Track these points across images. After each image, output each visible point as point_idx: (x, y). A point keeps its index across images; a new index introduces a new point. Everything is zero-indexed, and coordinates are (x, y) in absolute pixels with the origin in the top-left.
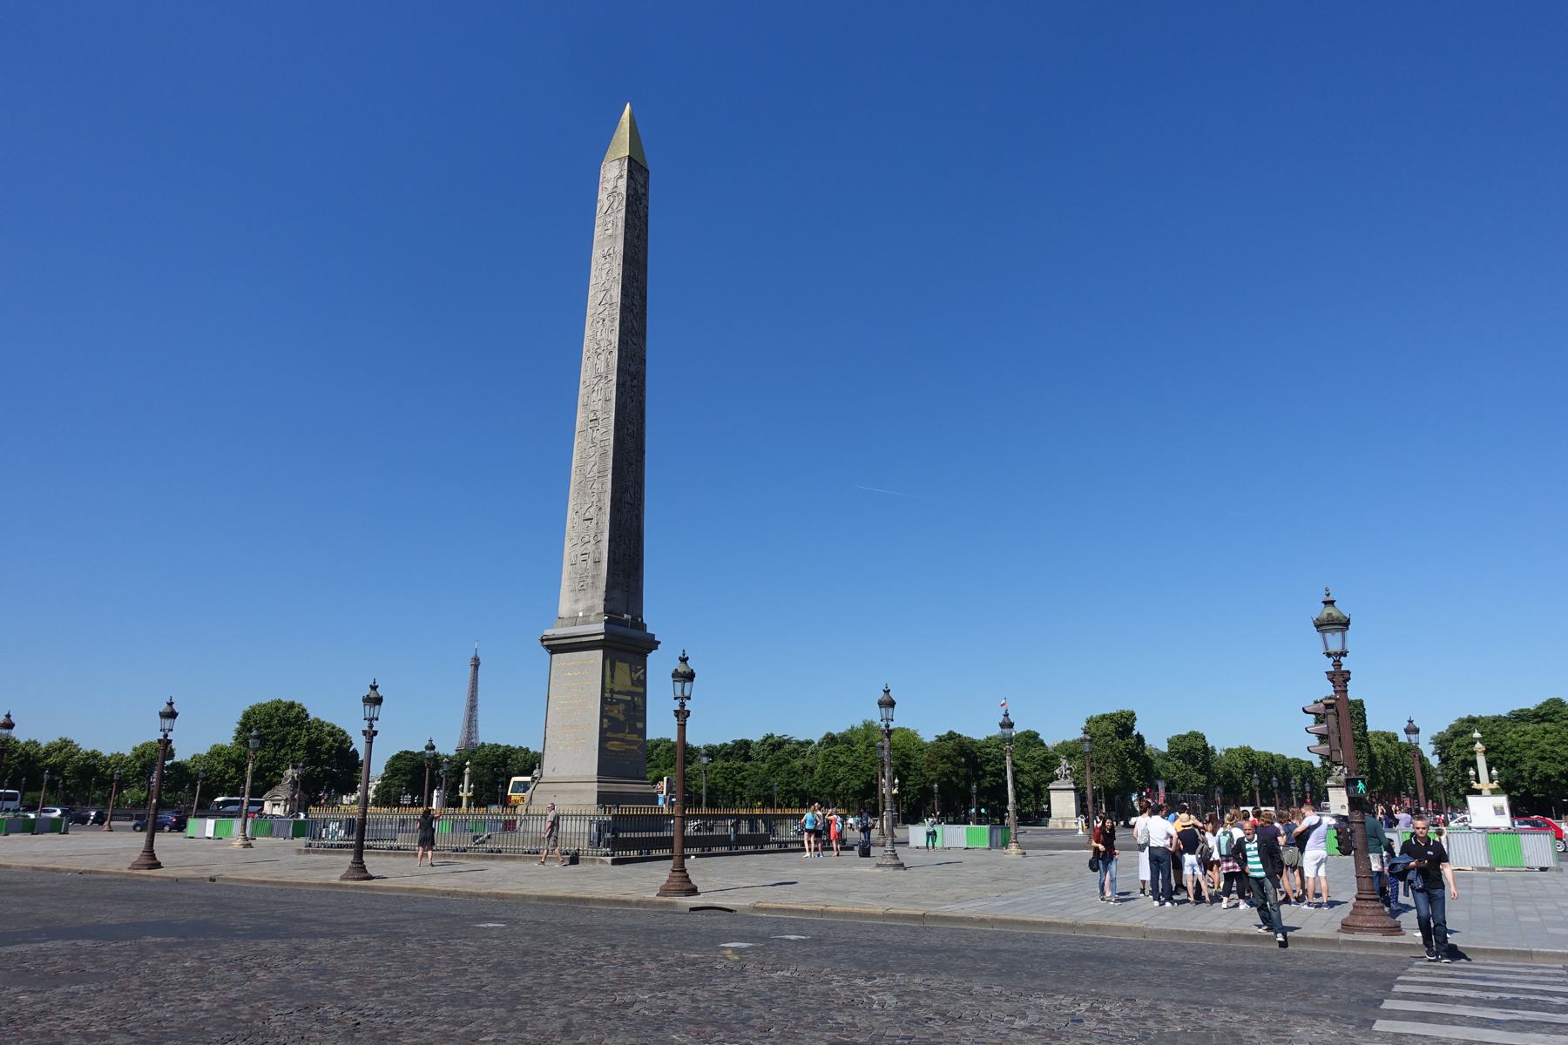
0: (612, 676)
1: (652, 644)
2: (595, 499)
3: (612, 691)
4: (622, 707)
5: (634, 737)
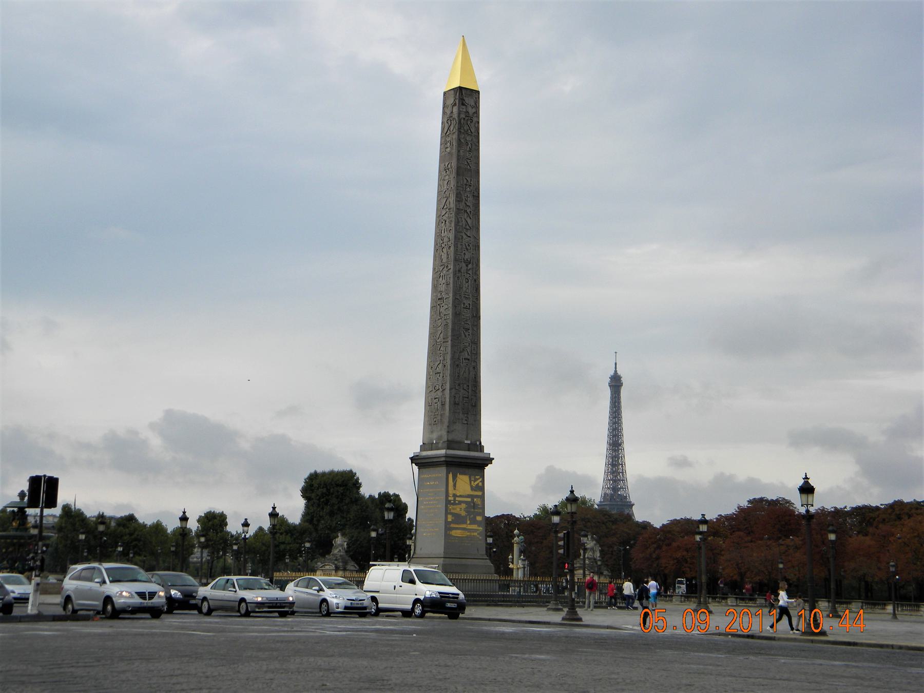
0: (455, 485)
1: (488, 460)
2: (442, 358)
3: (455, 496)
4: (464, 506)
5: (475, 527)
